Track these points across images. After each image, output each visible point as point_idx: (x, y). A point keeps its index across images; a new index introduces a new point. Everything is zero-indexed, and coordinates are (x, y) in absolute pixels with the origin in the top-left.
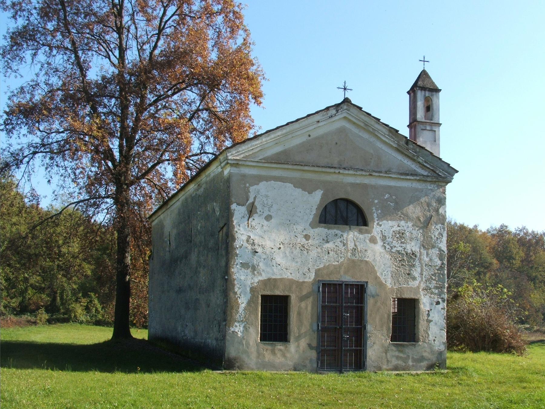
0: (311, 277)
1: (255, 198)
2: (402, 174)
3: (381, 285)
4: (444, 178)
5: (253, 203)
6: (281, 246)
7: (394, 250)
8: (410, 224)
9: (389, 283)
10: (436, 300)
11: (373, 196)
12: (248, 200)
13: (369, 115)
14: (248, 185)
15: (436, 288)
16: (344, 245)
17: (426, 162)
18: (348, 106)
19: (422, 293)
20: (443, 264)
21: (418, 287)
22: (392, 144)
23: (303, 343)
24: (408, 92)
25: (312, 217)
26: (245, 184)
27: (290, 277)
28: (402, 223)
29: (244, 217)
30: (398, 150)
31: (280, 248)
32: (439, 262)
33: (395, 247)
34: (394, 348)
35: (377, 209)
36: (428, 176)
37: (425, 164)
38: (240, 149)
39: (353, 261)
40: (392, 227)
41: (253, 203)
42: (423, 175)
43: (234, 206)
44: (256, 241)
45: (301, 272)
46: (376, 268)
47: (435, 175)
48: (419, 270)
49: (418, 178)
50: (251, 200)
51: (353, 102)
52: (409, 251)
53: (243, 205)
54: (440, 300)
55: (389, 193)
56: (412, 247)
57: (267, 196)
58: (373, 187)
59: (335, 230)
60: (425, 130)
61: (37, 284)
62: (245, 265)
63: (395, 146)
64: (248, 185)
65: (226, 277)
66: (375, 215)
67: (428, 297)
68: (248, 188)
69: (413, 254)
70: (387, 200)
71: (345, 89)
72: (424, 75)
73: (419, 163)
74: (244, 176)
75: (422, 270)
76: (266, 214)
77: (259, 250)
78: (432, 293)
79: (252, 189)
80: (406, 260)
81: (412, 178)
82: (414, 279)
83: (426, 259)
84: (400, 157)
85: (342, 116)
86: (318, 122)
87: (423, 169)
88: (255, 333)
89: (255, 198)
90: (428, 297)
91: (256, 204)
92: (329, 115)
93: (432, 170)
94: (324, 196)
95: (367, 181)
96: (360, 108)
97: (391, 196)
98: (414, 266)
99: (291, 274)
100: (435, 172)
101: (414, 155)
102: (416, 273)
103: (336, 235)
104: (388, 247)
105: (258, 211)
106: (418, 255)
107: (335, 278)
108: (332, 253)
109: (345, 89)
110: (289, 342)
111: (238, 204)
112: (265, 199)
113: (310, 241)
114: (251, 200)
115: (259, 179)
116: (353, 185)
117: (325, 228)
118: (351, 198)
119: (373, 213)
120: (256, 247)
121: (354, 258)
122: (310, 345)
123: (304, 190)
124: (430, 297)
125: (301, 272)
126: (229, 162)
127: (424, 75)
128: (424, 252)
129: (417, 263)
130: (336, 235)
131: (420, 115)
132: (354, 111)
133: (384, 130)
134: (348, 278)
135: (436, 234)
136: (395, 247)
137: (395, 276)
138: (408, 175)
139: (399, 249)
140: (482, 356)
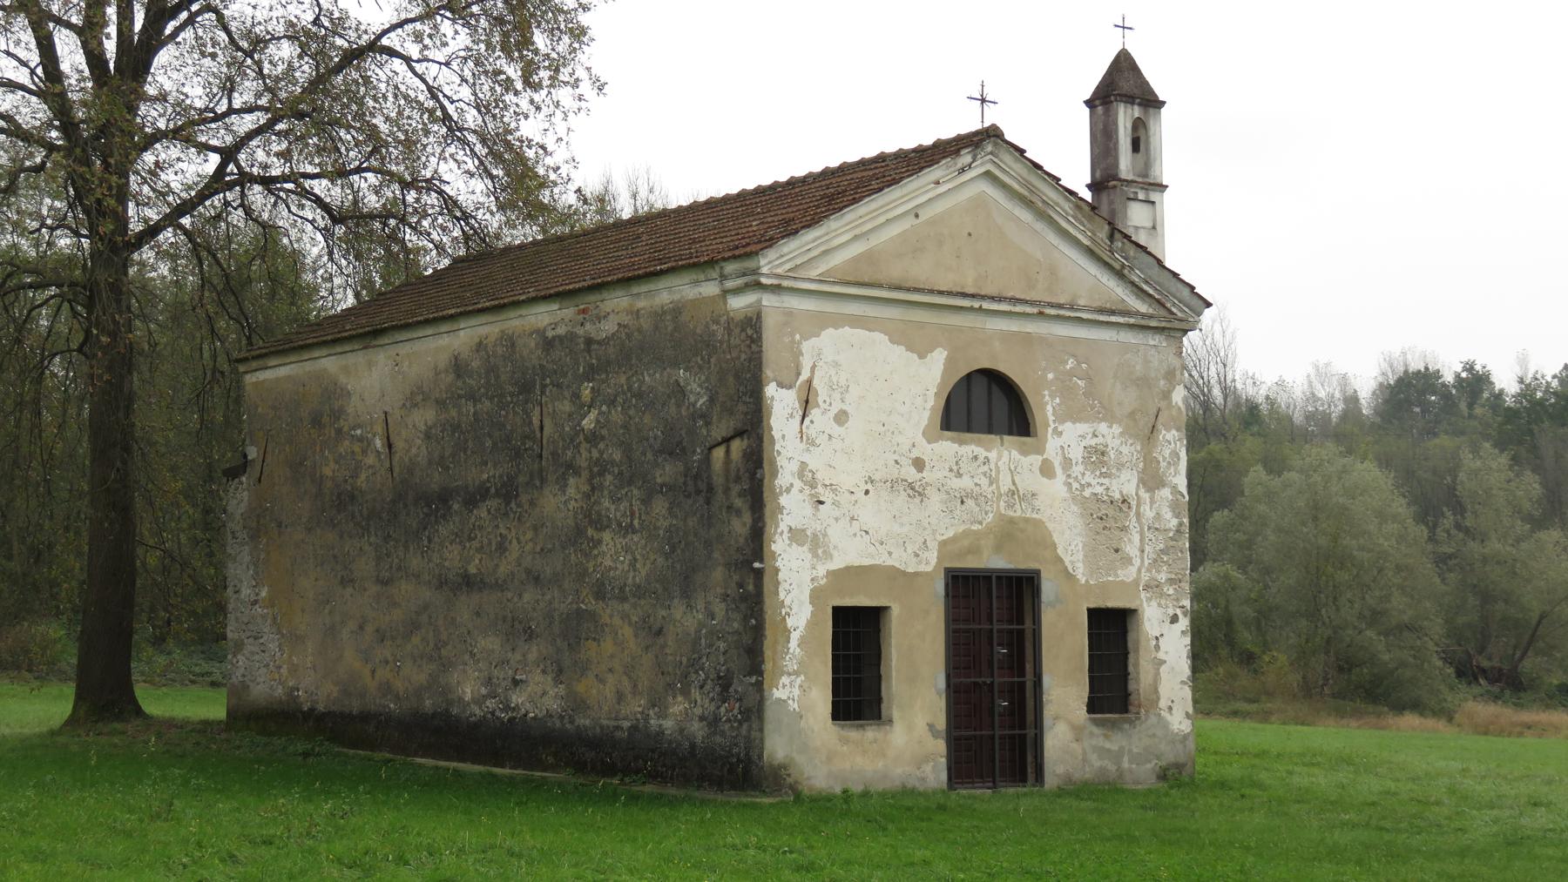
0: (930, 562)
1: (814, 367)
2: (1101, 311)
3: (1070, 577)
4: (1181, 320)
5: (810, 382)
6: (869, 487)
7: (1087, 493)
8: (1117, 429)
9: (1081, 574)
10: (1171, 612)
11: (1044, 364)
12: (799, 374)
13: (1039, 167)
14: (798, 337)
15: (1171, 581)
16: (991, 484)
17: (1147, 282)
18: (996, 144)
19: (1143, 595)
20: (1181, 524)
21: (1136, 582)
22: (1080, 237)
23: (921, 723)
24: (1089, 103)
25: (927, 414)
26: (792, 335)
27: (889, 562)
28: (1103, 427)
29: (791, 416)
30: (1090, 253)
31: (867, 492)
32: (1175, 522)
33: (1089, 485)
34: (1096, 730)
35: (1052, 397)
36: (1151, 317)
37: (1145, 287)
38: (785, 250)
39: (1012, 521)
40: (1083, 437)
41: (810, 382)
42: (1137, 313)
43: (771, 390)
44: (818, 476)
45: (909, 551)
46: (1056, 537)
47: (1163, 312)
48: (1136, 538)
49: (1132, 321)
50: (805, 376)
51: (1007, 137)
52: (1117, 496)
53: (790, 387)
54: (1178, 612)
55: (1074, 356)
56: (1126, 483)
57: (836, 364)
58: (1042, 340)
59: (973, 447)
60: (1136, 199)
61: (976, 527)
62: (797, 536)
63: (1086, 242)
64: (798, 337)
65: (757, 565)
66: (1049, 408)
67: (1154, 603)
68: (800, 343)
69: (1124, 501)
70: (1071, 374)
71: (983, 101)
72: (1123, 65)
73: (1133, 283)
74: (789, 313)
75: (1142, 540)
76: (834, 410)
77: (826, 496)
78: (1162, 595)
79: (807, 346)
80: (1107, 517)
81: (1121, 320)
82: (1128, 561)
83: (1149, 513)
84: (1093, 269)
85: (982, 170)
86: (938, 183)
87: (1138, 297)
88: (822, 699)
89: (814, 367)
90: (1154, 603)
91: (815, 383)
92: (959, 165)
93: (1158, 301)
94: (950, 363)
95: (1032, 327)
96: (1022, 152)
97: (1079, 363)
98: (1124, 529)
99: (890, 553)
100: (1163, 305)
101: (1123, 266)
102: (1132, 549)
103: (976, 458)
104: (1075, 485)
105: (820, 400)
106: (1134, 503)
107: (971, 563)
108: (970, 503)
109: (983, 101)
110: (891, 721)
111: (781, 385)
112: (832, 372)
113: (925, 474)
114: (805, 376)
115: (824, 322)
116: (1007, 337)
117: (953, 440)
118: (1002, 368)
119: (1045, 406)
120: (820, 489)
121: (1011, 514)
122: (931, 726)
123: (910, 349)
124: (1159, 605)
125: (909, 551)
126: (764, 280)
127: (1123, 65)
128: (1145, 496)
129: (1132, 522)
130: (976, 458)
131: (1126, 164)
132: (1008, 158)
133: (1067, 206)
134: (999, 562)
135: (1167, 452)
136: (1089, 485)
137: (1091, 554)
138: (1113, 312)
139: (1099, 490)
140: (1299, 728)
